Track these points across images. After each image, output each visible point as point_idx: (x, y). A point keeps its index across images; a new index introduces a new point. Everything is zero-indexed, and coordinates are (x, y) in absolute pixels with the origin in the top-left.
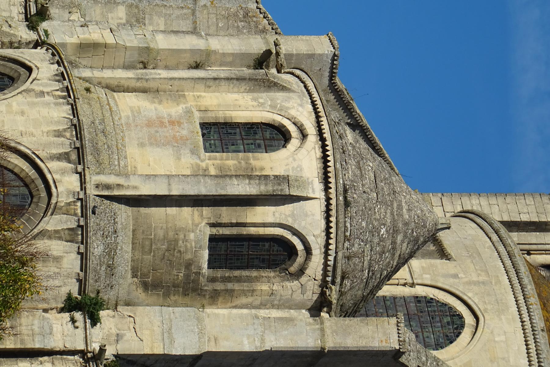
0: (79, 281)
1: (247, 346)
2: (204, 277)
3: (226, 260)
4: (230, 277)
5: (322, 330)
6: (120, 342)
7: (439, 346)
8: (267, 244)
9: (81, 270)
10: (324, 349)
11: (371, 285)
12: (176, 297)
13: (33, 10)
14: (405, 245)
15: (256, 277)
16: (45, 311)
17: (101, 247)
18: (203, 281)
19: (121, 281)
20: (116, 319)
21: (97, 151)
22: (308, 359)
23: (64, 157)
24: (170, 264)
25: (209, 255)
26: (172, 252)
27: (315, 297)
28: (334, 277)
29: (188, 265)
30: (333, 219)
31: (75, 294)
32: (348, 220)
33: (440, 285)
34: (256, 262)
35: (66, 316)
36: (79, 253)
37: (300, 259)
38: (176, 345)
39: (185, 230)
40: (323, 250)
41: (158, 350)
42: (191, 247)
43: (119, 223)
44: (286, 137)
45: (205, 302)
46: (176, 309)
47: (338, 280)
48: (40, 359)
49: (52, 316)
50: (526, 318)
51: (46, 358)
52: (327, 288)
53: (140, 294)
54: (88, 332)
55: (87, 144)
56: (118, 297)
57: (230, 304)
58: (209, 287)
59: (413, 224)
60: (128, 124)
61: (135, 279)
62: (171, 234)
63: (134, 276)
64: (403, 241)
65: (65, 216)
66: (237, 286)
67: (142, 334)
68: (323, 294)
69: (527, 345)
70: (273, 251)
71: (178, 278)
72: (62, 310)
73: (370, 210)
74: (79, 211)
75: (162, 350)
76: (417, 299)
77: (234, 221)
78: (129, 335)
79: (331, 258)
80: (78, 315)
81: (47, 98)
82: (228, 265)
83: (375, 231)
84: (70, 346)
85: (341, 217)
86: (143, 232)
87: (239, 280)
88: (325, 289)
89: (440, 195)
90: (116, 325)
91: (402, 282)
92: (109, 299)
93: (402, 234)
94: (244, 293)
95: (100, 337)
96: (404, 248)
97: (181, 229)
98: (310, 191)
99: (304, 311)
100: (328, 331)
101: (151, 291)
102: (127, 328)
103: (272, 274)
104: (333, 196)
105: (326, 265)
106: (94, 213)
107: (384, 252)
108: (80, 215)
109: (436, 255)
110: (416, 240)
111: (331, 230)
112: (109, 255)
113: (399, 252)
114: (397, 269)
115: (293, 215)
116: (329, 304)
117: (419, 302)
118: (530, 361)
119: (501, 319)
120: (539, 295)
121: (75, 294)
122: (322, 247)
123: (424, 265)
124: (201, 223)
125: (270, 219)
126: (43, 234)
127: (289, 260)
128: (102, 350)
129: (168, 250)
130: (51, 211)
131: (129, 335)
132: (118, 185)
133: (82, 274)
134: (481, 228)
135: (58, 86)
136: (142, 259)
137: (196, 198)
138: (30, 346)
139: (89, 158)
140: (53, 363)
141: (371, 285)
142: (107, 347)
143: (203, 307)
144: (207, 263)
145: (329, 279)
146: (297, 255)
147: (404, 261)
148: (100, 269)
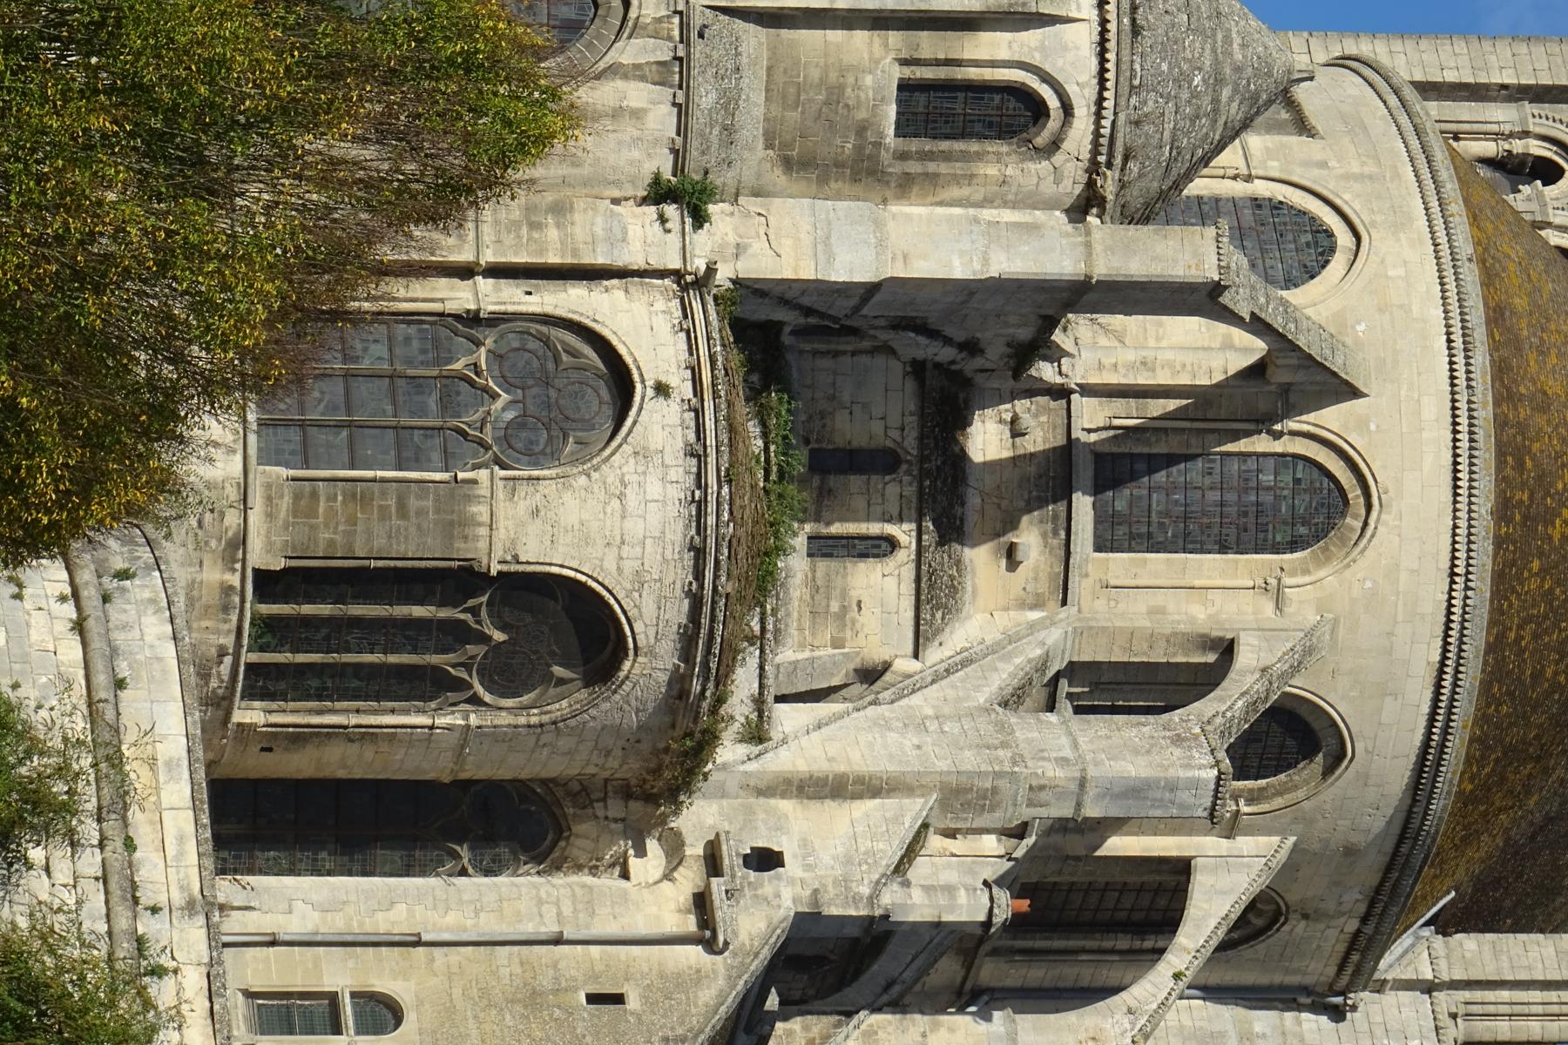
0: (675, 152)
1: (959, 271)
2: (887, 150)
3: (927, 121)
4: (932, 152)
5: (1088, 245)
6: (741, 258)
7: (1290, 283)
8: (997, 98)
9: (678, 134)
10: (1091, 278)
11: (1174, 172)
12: (840, 184)
14: (1235, 105)
15: (977, 153)
16: (616, 201)
17: (713, 96)
18: (885, 157)
19: (746, 154)
20: (736, 219)
22: (1064, 294)
24: (830, 127)
25: (898, 113)
26: (833, 107)
27: (1078, 189)
28: (1111, 155)
29: (861, 130)
30: (1111, 56)
31: (667, 174)
32: (1137, 58)
33: (1295, 179)
34: (978, 128)
36: (674, 104)
37: (1053, 124)
38: (837, 264)
39: (858, 70)
40: (1093, 109)
41: (808, 273)
42: (867, 99)
43: (745, 55)
45: (888, 194)
46: (839, 204)
47: (1118, 161)
48: (605, 283)
49: (627, 210)
50: (1443, 239)
51: (615, 282)
52: (1098, 174)
53: (777, 177)
54: (687, 238)
56: (739, 181)
57: (930, 199)
58: (897, 168)
59: (1250, 69)
61: (771, 152)
62: (833, 77)
63: (769, 146)
64: (1231, 99)
65: (653, 40)
66: (943, 168)
67: (780, 244)
68: (1091, 184)
69: (1442, 284)
70: (1007, 109)
71: (843, 152)
72: (644, 201)
73: (1176, 43)
74: (676, 33)
75: (813, 272)
76: (1256, 202)
77: (941, 56)
78: (758, 246)
79: (1106, 123)
80: (671, 210)
82: (929, 131)
83: (1183, 79)
84: (656, 263)
85: (1125, 53)
86: (785, 71)
87: (947, 157)
88: (1094, 176)
89: (1306, 34)
90: (735, 229)
91: (1231, 172)
92: (724, 184)
93: (1230, 87)
94: (956, 180)
95: (708, 248)
96: (1233, 111)
97: (850, 68)
98: (1074, 7)
99: (1057, 213)
100: (1098, 248)
101: (797, 173)
102: (753, 234)
103: (1005, 149)
104: (1112, 16)
105: (1097, 135)
106: (701, 36)
107: (1197, 117)
108: (678, 39)
109: (1292, 128)
110: (1255, 97)
111: (1107, 76)
112: (726, 109)
113: (1224, 118)
114: (1220, 148)
115: (1042, 48)
116: (1101, 202)
117: (1259, 207)
118: (1446, 312)
119: (1398, 240)
120: (1466, 201)
121: (667, 174)
122: (1092, 105)
123: (1270, 145)
124: (885, 58)
125: (1004, 55)
126: (614, 70)
127: (1035, 123)
128: (711, 270)
129: (827, 103)
130: (628, 31)
131: (758, 246)
133: (679, 141)
134: (1371, 85)
136: (783, 116)
137: (876, 15)
138: (587, 259)
140: (626, 291)
141: (1174, 172)
142: (718, 266)
143: (885, 201)
144: (893, 127)
145: (1102, 159)
146: (1048, 116)
147: (1234, 133)
148: (711, 133)
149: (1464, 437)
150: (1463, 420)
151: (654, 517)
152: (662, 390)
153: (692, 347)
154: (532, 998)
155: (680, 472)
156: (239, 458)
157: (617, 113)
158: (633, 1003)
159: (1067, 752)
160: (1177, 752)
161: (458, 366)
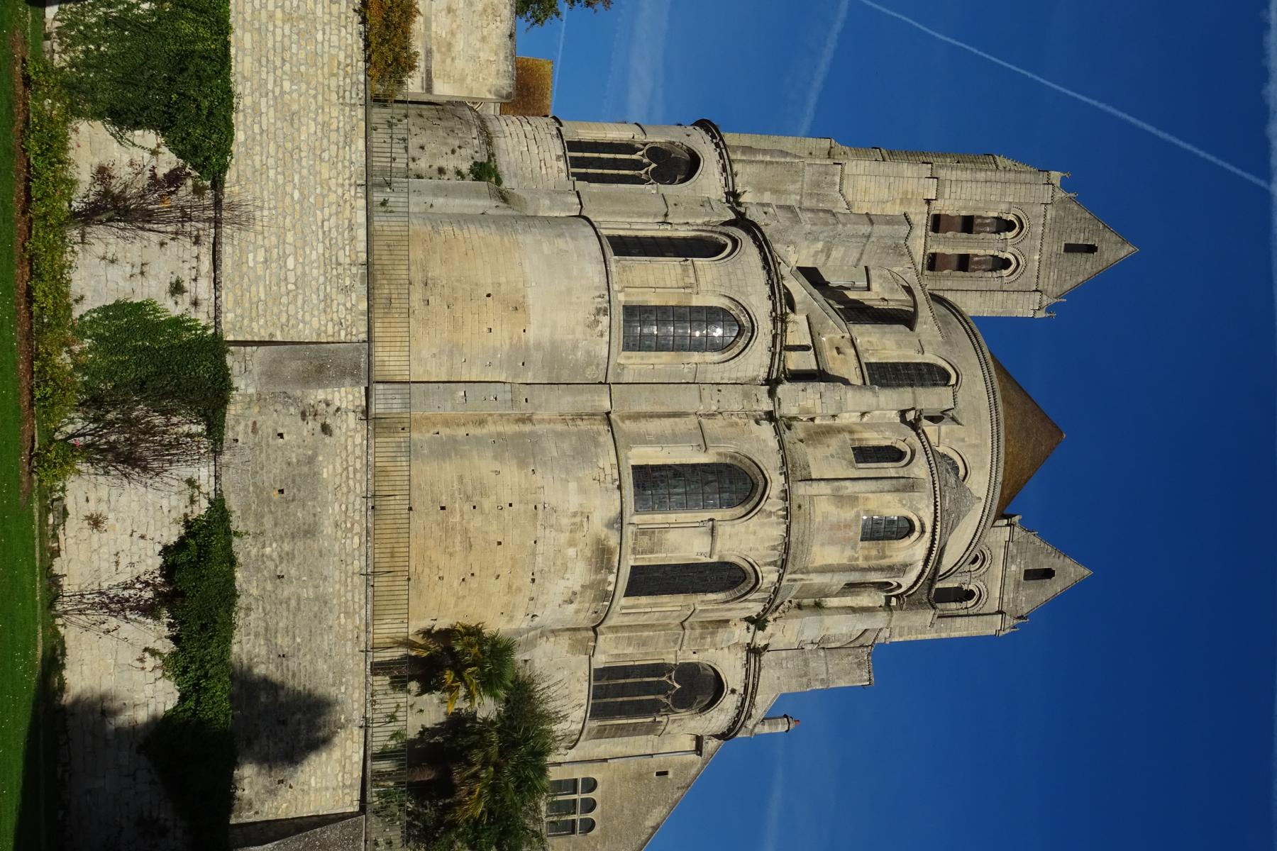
5: (890, 620)
13: (774, 376)
21: (795, 558)
23: (774, 563)
35: (745, 624)
39: (831, 586)
44: (911, 529)
50: (994, 476)
55: (790, 558)
60: (818, 529)
80: (752, 627)
81: (774, 518)
100: (893, 619)
126: (746, 600)
132: (802, 579)
135: (781, 504)
139: (789, 565)
149: (976, 539)
150: (979, 534)
151: (719, 724)
152: (733, 691)
153: (747, 676)
154: (639, 777)
155: (732, 713)
156: (581, 725)
157: (742, 609)
158: (670, 775)
159: (824, 676)
160: (858, 671)
161: (664, 679)
